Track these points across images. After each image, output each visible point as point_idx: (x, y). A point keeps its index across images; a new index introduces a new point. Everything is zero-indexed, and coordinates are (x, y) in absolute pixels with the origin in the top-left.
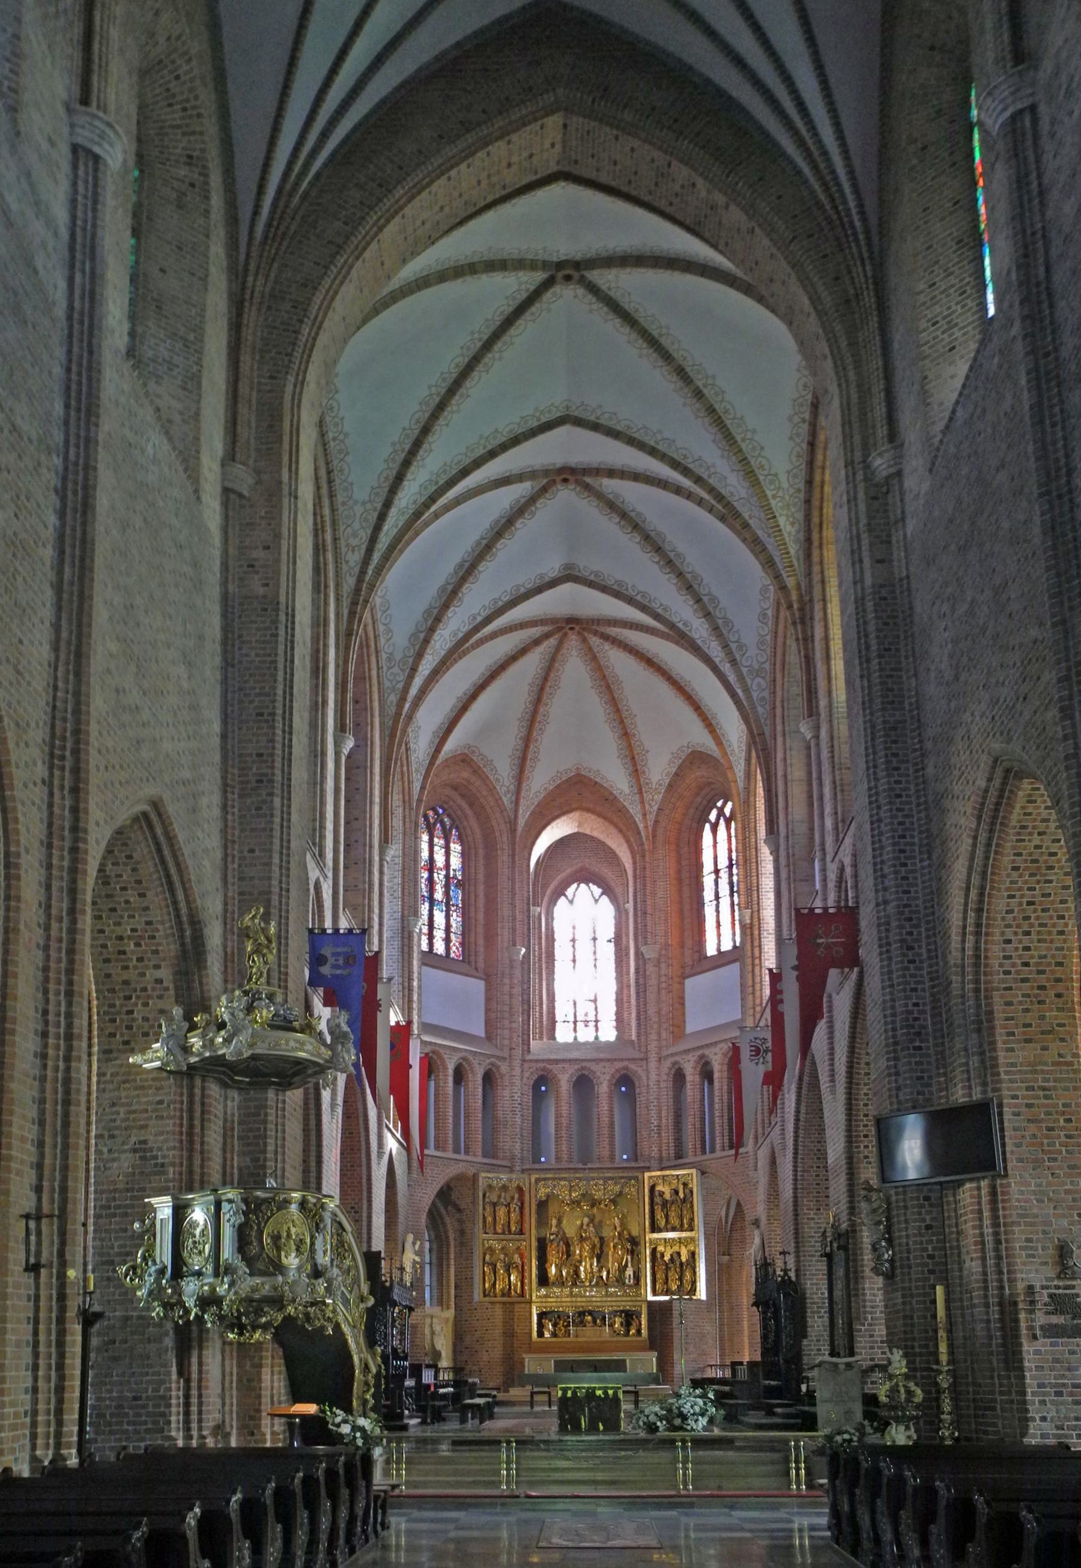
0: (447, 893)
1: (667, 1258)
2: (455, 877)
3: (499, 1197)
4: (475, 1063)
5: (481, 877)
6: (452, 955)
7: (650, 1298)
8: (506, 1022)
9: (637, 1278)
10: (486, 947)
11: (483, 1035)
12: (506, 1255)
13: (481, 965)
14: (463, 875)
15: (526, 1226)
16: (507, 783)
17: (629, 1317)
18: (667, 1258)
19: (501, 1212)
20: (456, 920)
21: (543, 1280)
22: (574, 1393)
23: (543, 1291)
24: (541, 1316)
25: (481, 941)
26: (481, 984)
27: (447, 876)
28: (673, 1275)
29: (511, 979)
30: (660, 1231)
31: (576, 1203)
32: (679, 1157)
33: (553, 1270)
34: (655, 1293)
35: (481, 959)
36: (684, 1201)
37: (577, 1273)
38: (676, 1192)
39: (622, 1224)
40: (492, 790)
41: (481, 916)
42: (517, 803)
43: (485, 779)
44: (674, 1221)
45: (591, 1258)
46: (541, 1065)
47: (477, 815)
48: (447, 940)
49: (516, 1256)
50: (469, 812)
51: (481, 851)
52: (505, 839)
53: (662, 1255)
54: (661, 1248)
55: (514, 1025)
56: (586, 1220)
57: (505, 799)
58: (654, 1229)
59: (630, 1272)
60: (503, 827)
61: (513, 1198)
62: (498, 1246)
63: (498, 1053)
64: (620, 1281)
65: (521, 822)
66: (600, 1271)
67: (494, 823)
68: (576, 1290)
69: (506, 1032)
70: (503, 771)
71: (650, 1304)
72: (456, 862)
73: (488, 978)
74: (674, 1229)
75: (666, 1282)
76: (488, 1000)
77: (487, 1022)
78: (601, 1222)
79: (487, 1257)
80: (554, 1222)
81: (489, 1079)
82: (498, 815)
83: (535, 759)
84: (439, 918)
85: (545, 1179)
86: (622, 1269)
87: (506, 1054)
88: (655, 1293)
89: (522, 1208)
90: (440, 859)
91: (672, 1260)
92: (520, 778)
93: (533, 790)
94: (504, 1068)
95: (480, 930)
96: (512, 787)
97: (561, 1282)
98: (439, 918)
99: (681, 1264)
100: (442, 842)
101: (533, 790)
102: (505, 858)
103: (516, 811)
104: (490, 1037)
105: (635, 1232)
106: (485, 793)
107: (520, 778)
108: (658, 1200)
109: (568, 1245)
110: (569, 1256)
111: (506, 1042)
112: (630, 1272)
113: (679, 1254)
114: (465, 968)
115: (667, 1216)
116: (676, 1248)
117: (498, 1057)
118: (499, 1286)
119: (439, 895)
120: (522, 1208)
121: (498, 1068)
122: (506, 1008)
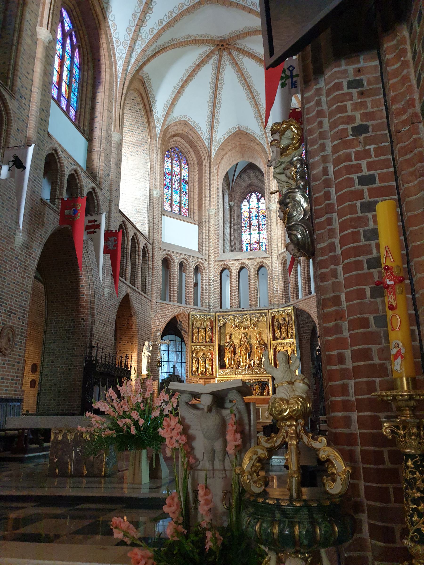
0: (180, 186)
2: (184, 179)
3: (201, 325)
4: (190, 261)
5: (196, 179)
6: (182, 214)
8: (207, 243)
10: (198, 210)
11: (197, 250)
12: (204, 354)
13: (196, 218)
14: (189, 179)
15: (214, 339)
16: (206, 134)
19: (202, 332)
20: (185, 199)
23: (222, 372)
25: (196, 208)
26: (197, 227)
27: (180, 178)
29: (209, 223)
30: (278, 339)
31: (237, 327)
33: (227, 361)
35: (196, 215)
36: (288, 323)
37: (239, 362)
38: (285, 319)
39: (260, 337)
40: (199, 138)
41: (196, 196)
42: (211, 144)
43: (196, 133)
44: (284, 334)
45: (246, 354)
46: (223, 263)
47: (194, 151)
48: (180, 207)
49: (209, 354)
50: (191, 150)
51: (196, 168)
52: (206, 160)
54: (278, 349)
55: (210, 244)
56: (243, 335)
57: (206, 142)
58: (275, 338)
60: (205, 155)
61: (207, 325)
62: (198, 348)
63: (203, 257)
65: (214, 153)
66: (250, 361)
67: (201, 153)
68: (237, 371)
69: (207, 248)
70: (203, 129)
72: (185, 173)
73: (200, 224)
74: (284, 338)
76: (199, 234)
77: (199, 244)
78: (250, 336)
79: (194, 355)
80: (228, 337)
81: (197, 269)
82: (203, 149)
83: (218, 122)
84: (176, 197)
85: (223, 315)
86: (260, 360)
87: (207, 258)
89: (212, 330)
90: (177, 170)
92: (211, 132)
93: (218, 138)
94: (205, 264)
95: (196, 203)
96: (208, 136)
98: (176, 197)
100: (178, 163)
101: (218, 138)
102: (206, 169)
103: (211, 147)
104: (199, 251)
105: (266, 342)
106: (196, 139)
107: (211, 132)
108: (276, 324)
109: (235, 349)
110: (235, 354)
111: (207, 252)
113: (287, 351)
114: (189, 220)
115: (281, 332)
116: (285, 348)
117: (202, 259)
118: (200, 369)
119: (176, 186)
120: (212, 330)
121: (202, 264)
122: (207, 237)
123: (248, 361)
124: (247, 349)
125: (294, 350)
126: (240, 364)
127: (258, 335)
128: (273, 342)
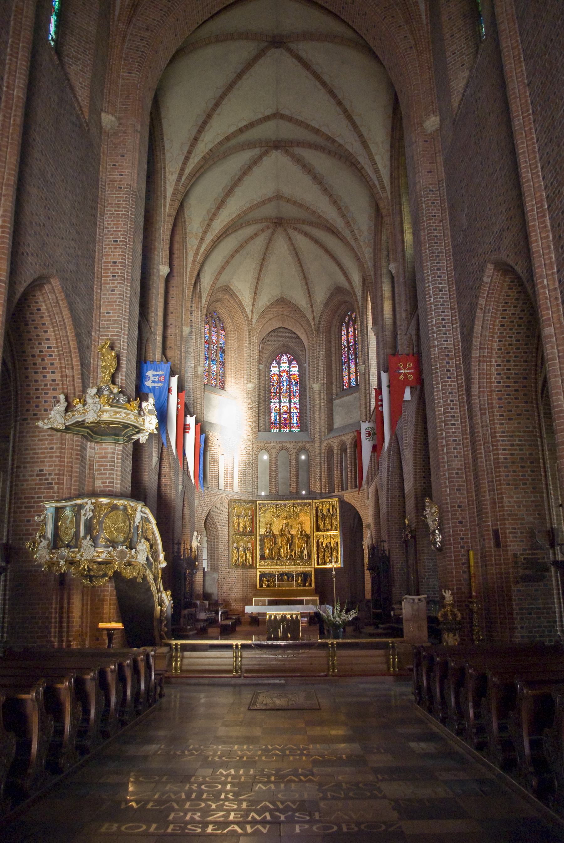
1: (324, 545)
7: (316, 566)
9: (309, 556)
17: (305, 576)
18: (324, 545)
21: (263, 557)
22: (275, 617)
23: (263, 563)
24: (262, 576)
28: (327, 554)
30: (321, 531)
32: (330, 494)
34: (318, 564)
36: (333, 515)
38: (329, 510)
44: (328, 526)
45: (287, 545)
53: (322, 544)
54: (321, 540)
58: (318, 530)
59: (306, 552)
64: (301, 557)
66: (291, 551)
68: (279, 562)
71: (316, 570)
74: (328, 530)
75: (324, 558)
86: (302, 552)
88: (318, 564)
91: (327, 546)
97: (271, 558)
99: (331, 548)
108: (320, 514)
109: (275, 539)
112: (306, 552)
113: (330, 543)
115: (324, 524)
116: (328, 540)
123: (289, 551)
124: (288, 539)
125: (337, 543)
126: (280, 556)
127: (300, 526)
128: (316, 533)
